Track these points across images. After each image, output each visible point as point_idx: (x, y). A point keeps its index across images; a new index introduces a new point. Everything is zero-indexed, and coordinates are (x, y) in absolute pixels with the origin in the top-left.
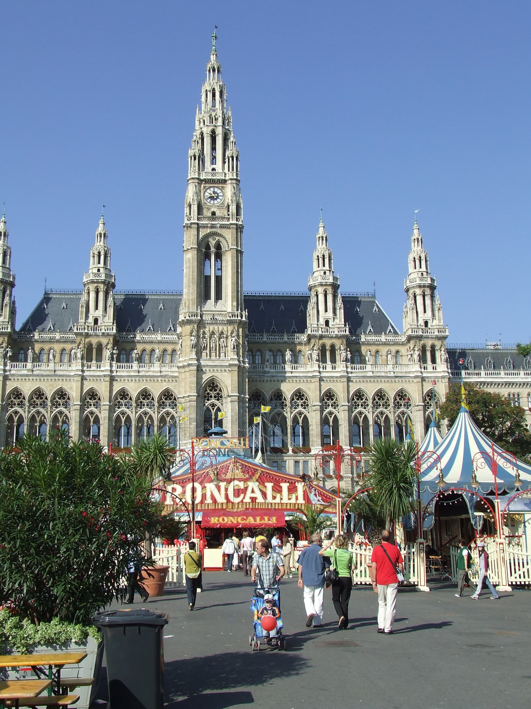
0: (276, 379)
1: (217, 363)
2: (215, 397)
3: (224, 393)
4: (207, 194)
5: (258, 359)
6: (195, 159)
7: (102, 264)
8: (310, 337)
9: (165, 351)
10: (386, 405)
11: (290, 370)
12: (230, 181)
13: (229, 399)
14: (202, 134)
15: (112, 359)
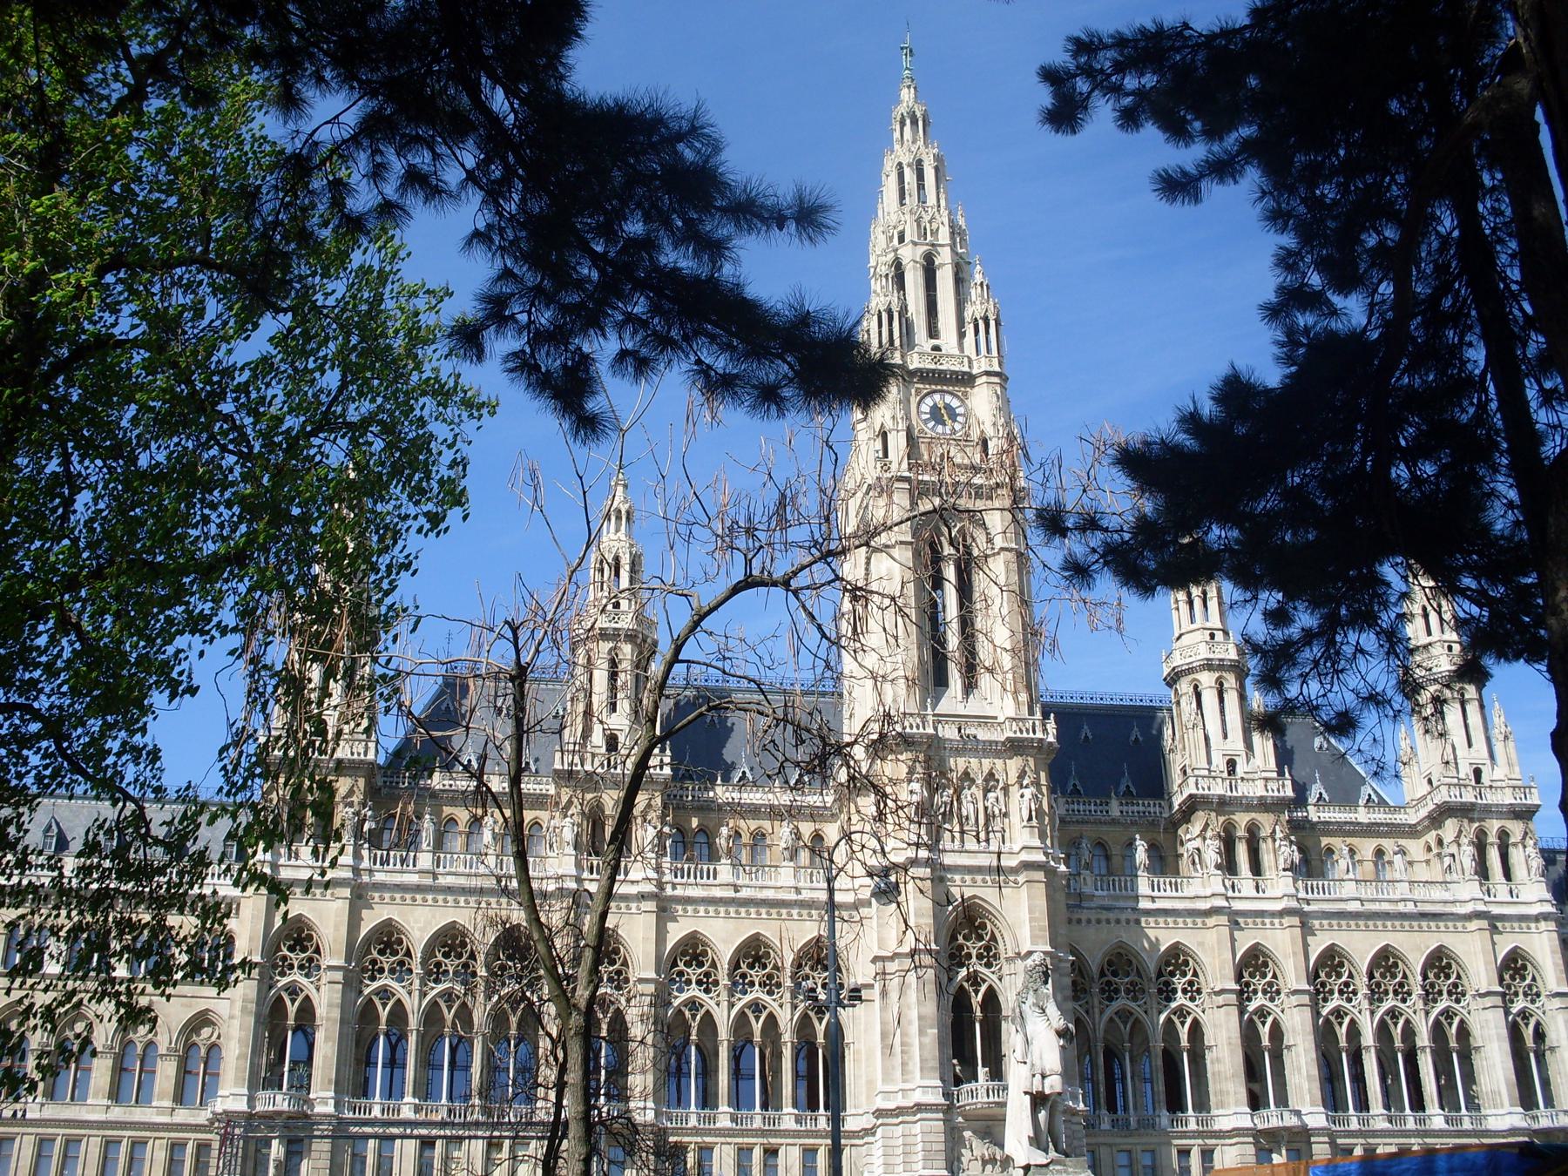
0: (1111, 916)
3: (1006, 948)
10: (1402, 992)
12: (984, 379)
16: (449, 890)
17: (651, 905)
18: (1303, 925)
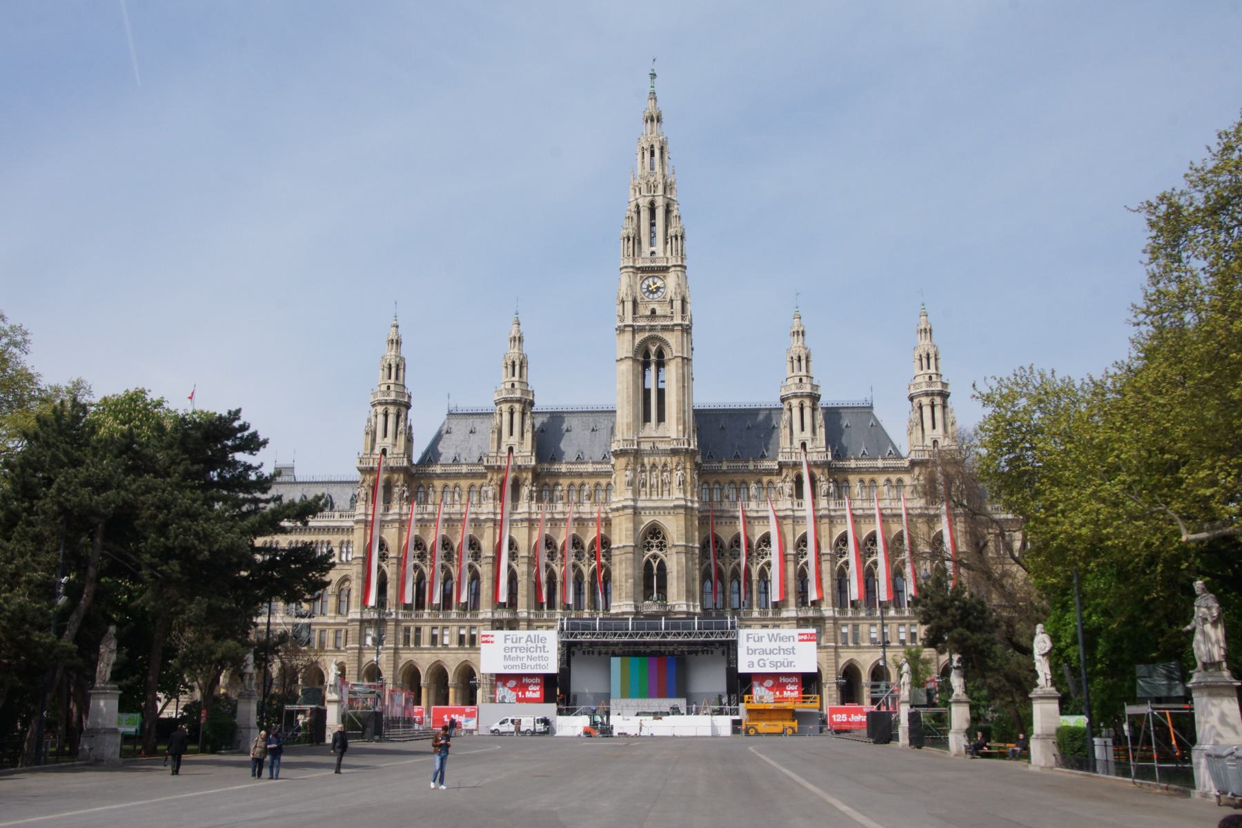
3: (669, 543)
5: (716, 497)
7: (517, 378)
8: (782, 466)
9: (598, 484)
13: (674, 550)
14: (638, 206)
15: (532, 499)
17: (526, 524)
18: (831, 522)
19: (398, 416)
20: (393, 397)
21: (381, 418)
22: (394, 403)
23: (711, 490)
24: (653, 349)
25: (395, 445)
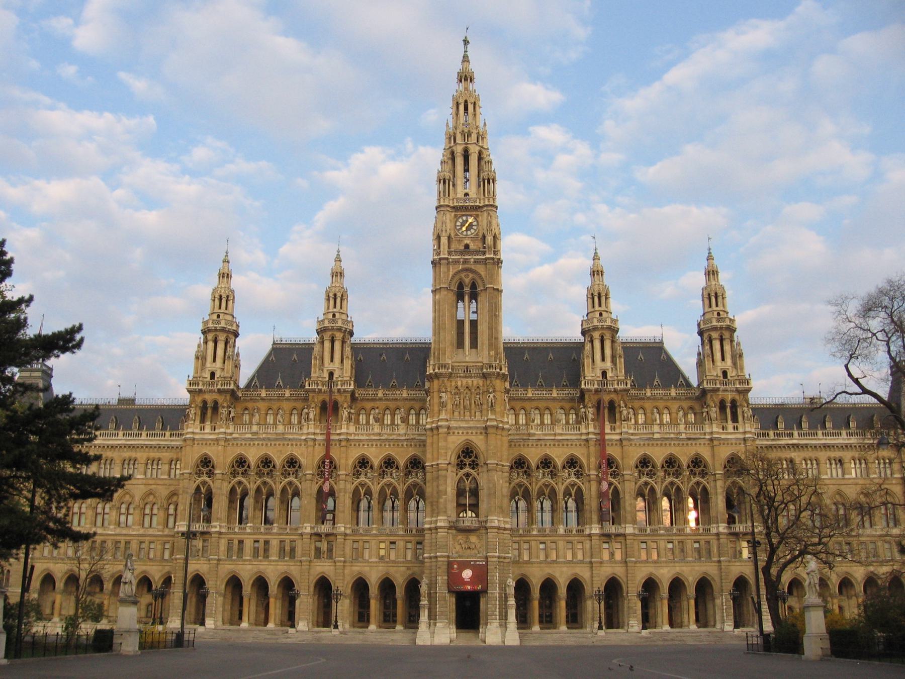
0: (543, 443)
1: (471, 424)
2: (470, 465)
3: (481, 461)
4: (458, 224)
6: (444, 182)
8: (583, 393)
11: (561, 432)
13: (485, 469)
14: (453, 153)
15: (350, 419)
16: (264, 439)
19: (226, 343)
20: (223, 324)
21: (211, 345)
22: (223, 330)
23: (517, 415)
24: (467, 281)
25: (223, 369)
